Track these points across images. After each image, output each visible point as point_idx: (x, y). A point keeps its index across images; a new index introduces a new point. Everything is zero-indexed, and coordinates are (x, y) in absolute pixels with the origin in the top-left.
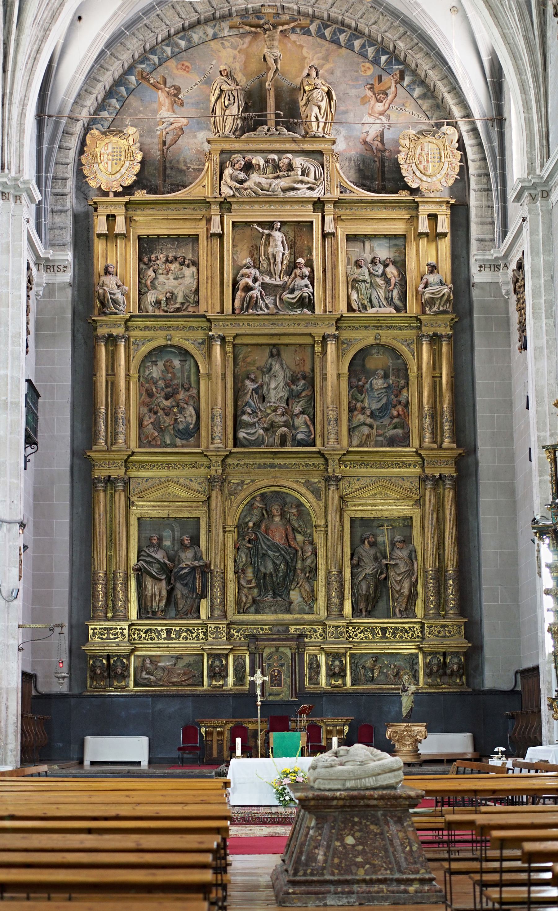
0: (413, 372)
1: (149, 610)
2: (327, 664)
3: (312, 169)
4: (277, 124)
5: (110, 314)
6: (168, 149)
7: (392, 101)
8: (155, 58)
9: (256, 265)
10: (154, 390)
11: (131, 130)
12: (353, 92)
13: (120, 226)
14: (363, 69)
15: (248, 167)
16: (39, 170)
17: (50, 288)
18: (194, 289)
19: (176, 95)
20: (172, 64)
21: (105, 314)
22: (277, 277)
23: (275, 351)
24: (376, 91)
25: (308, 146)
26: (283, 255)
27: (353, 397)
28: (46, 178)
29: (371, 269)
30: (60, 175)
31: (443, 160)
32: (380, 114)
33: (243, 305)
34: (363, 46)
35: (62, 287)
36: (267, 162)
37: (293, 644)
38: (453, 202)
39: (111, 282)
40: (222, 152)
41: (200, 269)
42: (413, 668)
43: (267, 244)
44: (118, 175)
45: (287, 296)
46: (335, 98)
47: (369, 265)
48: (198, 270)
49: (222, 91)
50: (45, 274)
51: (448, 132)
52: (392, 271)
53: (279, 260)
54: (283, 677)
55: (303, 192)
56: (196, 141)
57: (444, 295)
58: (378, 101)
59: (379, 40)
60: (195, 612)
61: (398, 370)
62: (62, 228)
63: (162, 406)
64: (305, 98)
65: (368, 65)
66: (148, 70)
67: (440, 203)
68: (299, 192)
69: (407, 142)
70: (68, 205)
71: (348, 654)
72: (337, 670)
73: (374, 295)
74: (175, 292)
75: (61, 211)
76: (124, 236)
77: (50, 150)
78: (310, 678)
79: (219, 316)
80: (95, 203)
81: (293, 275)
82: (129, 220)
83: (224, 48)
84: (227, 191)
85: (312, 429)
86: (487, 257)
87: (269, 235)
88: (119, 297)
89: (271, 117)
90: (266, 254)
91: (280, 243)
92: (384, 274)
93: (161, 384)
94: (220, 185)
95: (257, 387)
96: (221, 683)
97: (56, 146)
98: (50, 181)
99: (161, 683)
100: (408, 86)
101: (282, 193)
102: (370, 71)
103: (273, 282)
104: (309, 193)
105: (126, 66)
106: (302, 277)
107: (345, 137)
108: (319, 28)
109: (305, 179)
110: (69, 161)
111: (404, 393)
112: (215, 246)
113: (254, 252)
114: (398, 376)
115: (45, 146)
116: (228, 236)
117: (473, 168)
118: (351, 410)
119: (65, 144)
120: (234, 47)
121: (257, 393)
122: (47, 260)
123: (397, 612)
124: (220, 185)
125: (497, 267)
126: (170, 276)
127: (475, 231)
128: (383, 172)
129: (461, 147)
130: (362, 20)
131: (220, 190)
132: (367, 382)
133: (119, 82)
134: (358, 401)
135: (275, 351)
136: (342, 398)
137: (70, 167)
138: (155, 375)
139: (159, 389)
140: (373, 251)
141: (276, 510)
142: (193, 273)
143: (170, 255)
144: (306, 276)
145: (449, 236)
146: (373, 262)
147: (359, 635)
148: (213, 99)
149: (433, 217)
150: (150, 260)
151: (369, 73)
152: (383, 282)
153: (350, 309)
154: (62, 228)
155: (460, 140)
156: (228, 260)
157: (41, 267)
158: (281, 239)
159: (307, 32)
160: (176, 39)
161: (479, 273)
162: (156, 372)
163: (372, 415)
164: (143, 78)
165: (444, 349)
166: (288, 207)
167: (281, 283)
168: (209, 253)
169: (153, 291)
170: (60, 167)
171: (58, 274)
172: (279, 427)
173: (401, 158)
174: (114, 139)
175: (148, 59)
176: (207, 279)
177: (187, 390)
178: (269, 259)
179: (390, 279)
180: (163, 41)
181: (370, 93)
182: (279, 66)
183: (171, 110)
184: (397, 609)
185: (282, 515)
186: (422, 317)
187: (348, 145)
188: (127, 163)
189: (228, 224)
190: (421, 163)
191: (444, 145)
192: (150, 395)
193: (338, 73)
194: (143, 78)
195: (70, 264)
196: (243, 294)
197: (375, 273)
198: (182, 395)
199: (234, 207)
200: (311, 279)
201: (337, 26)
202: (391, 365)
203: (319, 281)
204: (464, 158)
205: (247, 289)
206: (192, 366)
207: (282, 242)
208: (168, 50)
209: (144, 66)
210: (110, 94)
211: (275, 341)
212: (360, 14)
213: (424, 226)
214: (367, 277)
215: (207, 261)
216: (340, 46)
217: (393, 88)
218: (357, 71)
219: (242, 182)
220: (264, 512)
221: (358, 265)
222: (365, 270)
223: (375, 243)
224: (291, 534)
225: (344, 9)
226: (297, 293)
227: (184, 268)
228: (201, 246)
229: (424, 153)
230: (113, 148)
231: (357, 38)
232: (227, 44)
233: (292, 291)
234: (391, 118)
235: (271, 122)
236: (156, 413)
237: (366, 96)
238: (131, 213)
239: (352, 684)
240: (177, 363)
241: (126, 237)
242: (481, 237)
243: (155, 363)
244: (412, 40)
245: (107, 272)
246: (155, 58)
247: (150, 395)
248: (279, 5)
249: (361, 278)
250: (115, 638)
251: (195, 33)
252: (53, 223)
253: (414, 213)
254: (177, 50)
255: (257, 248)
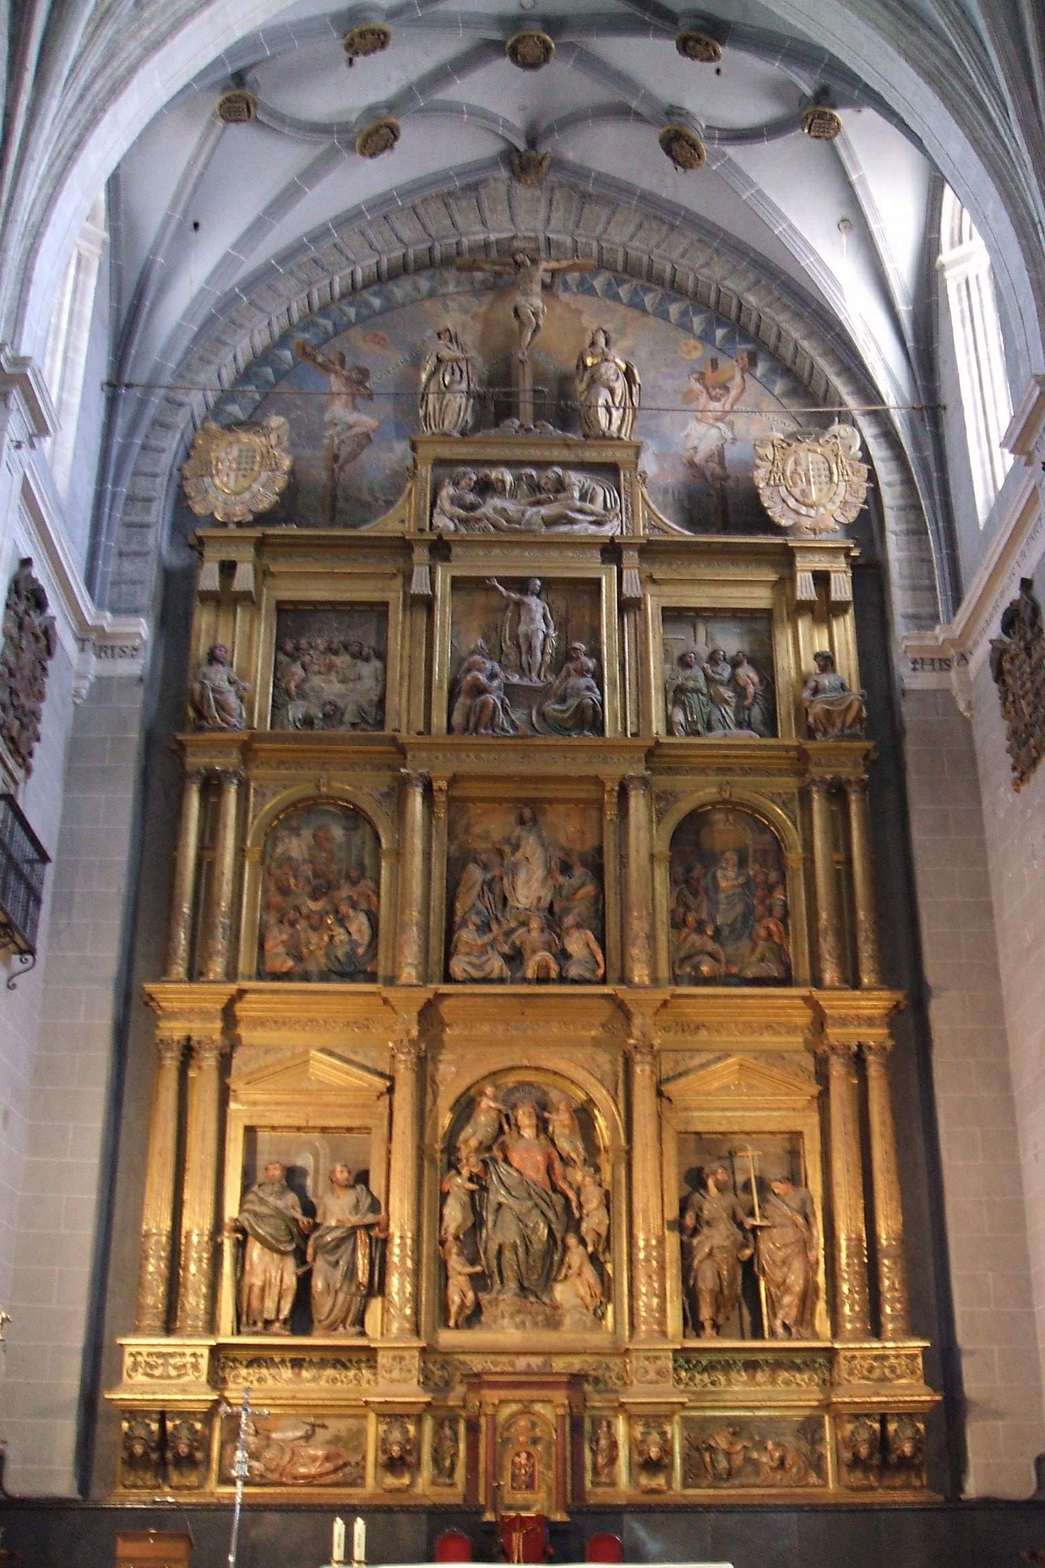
0: (794, 857)
1: (256, 1316)
2: (632, 1442)
3: (600, 491)
4: (538, 415)
5: (213, 730)
6: (341, 468)
7: (737, 399)
8: (328, 324)
9: (497, 653)
10: (292, 881)
11: (276, 421)
12: (668, 385)
13: (244, 579)
14: (685, 349)
15: (485, 488)
16: (102, 479)
17: (103, 685)
18: (376, 699)
19: (361, 383)
20: (356, 334)
21: (200, 729)
22: (534, 675)
23: (527, 813)
24: (709, 384)
25: (591, 455)
26: (546, 636)
27: (680, 900)
28: (114, 495)
29: (710, 671)
30: (141, 493)
31: (835, 478)
32: (717, 419)
33: (468, 721)
34: (684, 314)
35: (126, 683)
36: (518, 479)
37: (561, 1396)
38: (854, 553)
39: (219, 676)
40: (439, 463)
41: (390, 661)
42: (813, 1451)
43: (517, 621)
44: (247, 496)
45: (552, 707)
46: (638, 379)
47: (705, 665)
48: (385, 667)
49: (439, 360)
50: (94, 658)
51: (842, 433)
52: (747, 674)
53: (538, 642)
54: (539, 1468)
55: (584, 528)
56: (392, 455)
57: (850, 706)
58: (712, 398)
59: (713, 298)
60: (353, 1324)
61: (765, 852)
62: (134, 583)
63: (304, 911)
64: (585, 378)
65: (692, 342)
66: (314, 342)
67: (833, 551)
68: (576, 527)
69: (769, 452)
70: (151, 541)
71: (677, 1418)
72: (654, 1452)
73: (716, 715)
74: (341, 704)
75: (137, 554)
76: (248, 599)
77: (125, 449)
78: (596, 1471)
79: (421, 739)
80: (201, 540)
81: (563, 673)
82: (263, 574)
83: (447, 311)
84: (443, 523)
85: (600, 957)
86: (928, 643)
87: (519, 605)
88: (233, 701)
89: (527, 409)
90: (515, 637)
91: (539, 617)
92: (733, 681)
93: (307, 869)
94: (431, 515)
95: (493, 879)
96: (406, 1480)
97: (138, 441)
98: (120, 503)
99: (274, 1477)
100: (764, 376)
101: (543, 530)
102: (695, 352)
103: (526, 682)
104: (593, 529)
105: (277, 330)
106: (582, 672)
107: (656, 456)
108: (609, 284)
109: (588, 506)
110: (158, 470)
111: (779, 895)
112: (419, 621)
113: (492, 633)
114: (764, 864)
115: (118, 440)
116: (443, 602)
117: (890, 497)
118: (677, 924)
119: (153, 442)
120: (465, 311)
121: (490, 890)
122: (100, 630)
123: (780, 1330)
124: (431, 515)
125: (944, 664)
126: (333, 677)
127: (900, 601)
128: (725, 513)
129: (867, 458)
130: (684, 261)
131: (431, 523)
132: (705, 874)
133: (262, 358)
134: (688, 908)
135: (527, 813)
136: (658, 897)
137: (162, 481)
138: (295, 853)
139: (301, 879)
140: (712, 640)
141: (525, 1119)
142: (376, 669)
143: (336, 640)
144: (588, 671)
145: (851, 611)
146: (713, 658)
147: (698, 1377)
148: (424, 377)
149: (822, 579)
150: (297, 648)
151: (696, 355)
152: (731, 694)
153: (670, 731)
154: (134, 583)
155: (864, 447)
156: (442, 643)
157: (89, 645)
158: (541, 610)
159: (591, 291)
160: (366, 295)
161: (911, 673)
162: (296, 847)
163: (717, 936)
164: (305, 354)
165: (854, 809)
166: (555, 554)
167: (541, 685)
168: (407, 633)
169: (301, 702)
170: (143, 482)
171: (120, 661)
172: (534, 952)
173: (760, 478)
174: (244, 437)
175: (315, 324)
176: (402, 677)
177: (354, 883)
178: (518, 646)
179: (744, 689)
180: (343, 296)
181: (697, 387)
182: (541, 322)
183: (350, 405)
184: (778, 1323)
185: (542, 1126)
186: (809, 745)
187: (661, 468)
188: (264, 475)
189: (444, 581)
190: (795, 484)
191: (836, 456)
192: (284, 891)
193: (643, 353)
194: (305, 354)
195: (144, 643)
196: (468, 702)
197: (717, 677)
198: (345, 891)
199: (457, 551)
200: (598, 676)
201: (639, 282)
202: (749, 842)
203: (612, 683)
204: (872, 476)
205: (478, 690)
206: (367, 838)
207: (544, 617)
208: (351, 312)
209: (307, 336)
210: (245, 376)
211: (529, 792)
212: (680, 250)
213: (805, 590)
214: (702, 683)
215: (402, 647)
216: (644, 311)
217: (738, 379)
218: (675, 352)
219: (472, 507)
220: (504, 1121)
221: (684, 662)
222: (697, 672)
223: (717, 628)
224: (557, 1165)
225: (653, 242)
226: (573, 703)
227: (359, 663)
228: (391, 622)
229: (800, 470)
230: (241, 451)
231: (674, 300)
232: (452, 305)
233: (563, 699)
234: (736, 427)
235: (527, 409)
236: (292, 924)
237: (691, 391)
238: (266, 560)
239: (685, 1485)
240: (337, 832)
241: (253, 603)
242: (911, 611)
243: (296, 831)
244: (770, 292)
245: (213, 658)
246: (328, 324)
247: (284, 891)
248: (541, 237)
249: (691, 684)
250: (179, 1376)
251: (398, 286)
252: (119, 574)
253: (786, 572)
254: (365, 312)
255: (498, 628)
